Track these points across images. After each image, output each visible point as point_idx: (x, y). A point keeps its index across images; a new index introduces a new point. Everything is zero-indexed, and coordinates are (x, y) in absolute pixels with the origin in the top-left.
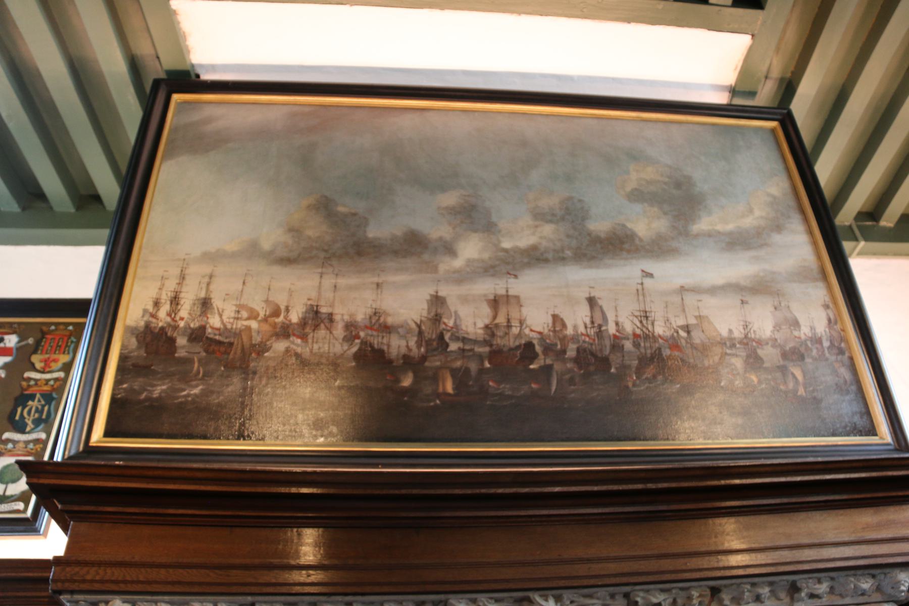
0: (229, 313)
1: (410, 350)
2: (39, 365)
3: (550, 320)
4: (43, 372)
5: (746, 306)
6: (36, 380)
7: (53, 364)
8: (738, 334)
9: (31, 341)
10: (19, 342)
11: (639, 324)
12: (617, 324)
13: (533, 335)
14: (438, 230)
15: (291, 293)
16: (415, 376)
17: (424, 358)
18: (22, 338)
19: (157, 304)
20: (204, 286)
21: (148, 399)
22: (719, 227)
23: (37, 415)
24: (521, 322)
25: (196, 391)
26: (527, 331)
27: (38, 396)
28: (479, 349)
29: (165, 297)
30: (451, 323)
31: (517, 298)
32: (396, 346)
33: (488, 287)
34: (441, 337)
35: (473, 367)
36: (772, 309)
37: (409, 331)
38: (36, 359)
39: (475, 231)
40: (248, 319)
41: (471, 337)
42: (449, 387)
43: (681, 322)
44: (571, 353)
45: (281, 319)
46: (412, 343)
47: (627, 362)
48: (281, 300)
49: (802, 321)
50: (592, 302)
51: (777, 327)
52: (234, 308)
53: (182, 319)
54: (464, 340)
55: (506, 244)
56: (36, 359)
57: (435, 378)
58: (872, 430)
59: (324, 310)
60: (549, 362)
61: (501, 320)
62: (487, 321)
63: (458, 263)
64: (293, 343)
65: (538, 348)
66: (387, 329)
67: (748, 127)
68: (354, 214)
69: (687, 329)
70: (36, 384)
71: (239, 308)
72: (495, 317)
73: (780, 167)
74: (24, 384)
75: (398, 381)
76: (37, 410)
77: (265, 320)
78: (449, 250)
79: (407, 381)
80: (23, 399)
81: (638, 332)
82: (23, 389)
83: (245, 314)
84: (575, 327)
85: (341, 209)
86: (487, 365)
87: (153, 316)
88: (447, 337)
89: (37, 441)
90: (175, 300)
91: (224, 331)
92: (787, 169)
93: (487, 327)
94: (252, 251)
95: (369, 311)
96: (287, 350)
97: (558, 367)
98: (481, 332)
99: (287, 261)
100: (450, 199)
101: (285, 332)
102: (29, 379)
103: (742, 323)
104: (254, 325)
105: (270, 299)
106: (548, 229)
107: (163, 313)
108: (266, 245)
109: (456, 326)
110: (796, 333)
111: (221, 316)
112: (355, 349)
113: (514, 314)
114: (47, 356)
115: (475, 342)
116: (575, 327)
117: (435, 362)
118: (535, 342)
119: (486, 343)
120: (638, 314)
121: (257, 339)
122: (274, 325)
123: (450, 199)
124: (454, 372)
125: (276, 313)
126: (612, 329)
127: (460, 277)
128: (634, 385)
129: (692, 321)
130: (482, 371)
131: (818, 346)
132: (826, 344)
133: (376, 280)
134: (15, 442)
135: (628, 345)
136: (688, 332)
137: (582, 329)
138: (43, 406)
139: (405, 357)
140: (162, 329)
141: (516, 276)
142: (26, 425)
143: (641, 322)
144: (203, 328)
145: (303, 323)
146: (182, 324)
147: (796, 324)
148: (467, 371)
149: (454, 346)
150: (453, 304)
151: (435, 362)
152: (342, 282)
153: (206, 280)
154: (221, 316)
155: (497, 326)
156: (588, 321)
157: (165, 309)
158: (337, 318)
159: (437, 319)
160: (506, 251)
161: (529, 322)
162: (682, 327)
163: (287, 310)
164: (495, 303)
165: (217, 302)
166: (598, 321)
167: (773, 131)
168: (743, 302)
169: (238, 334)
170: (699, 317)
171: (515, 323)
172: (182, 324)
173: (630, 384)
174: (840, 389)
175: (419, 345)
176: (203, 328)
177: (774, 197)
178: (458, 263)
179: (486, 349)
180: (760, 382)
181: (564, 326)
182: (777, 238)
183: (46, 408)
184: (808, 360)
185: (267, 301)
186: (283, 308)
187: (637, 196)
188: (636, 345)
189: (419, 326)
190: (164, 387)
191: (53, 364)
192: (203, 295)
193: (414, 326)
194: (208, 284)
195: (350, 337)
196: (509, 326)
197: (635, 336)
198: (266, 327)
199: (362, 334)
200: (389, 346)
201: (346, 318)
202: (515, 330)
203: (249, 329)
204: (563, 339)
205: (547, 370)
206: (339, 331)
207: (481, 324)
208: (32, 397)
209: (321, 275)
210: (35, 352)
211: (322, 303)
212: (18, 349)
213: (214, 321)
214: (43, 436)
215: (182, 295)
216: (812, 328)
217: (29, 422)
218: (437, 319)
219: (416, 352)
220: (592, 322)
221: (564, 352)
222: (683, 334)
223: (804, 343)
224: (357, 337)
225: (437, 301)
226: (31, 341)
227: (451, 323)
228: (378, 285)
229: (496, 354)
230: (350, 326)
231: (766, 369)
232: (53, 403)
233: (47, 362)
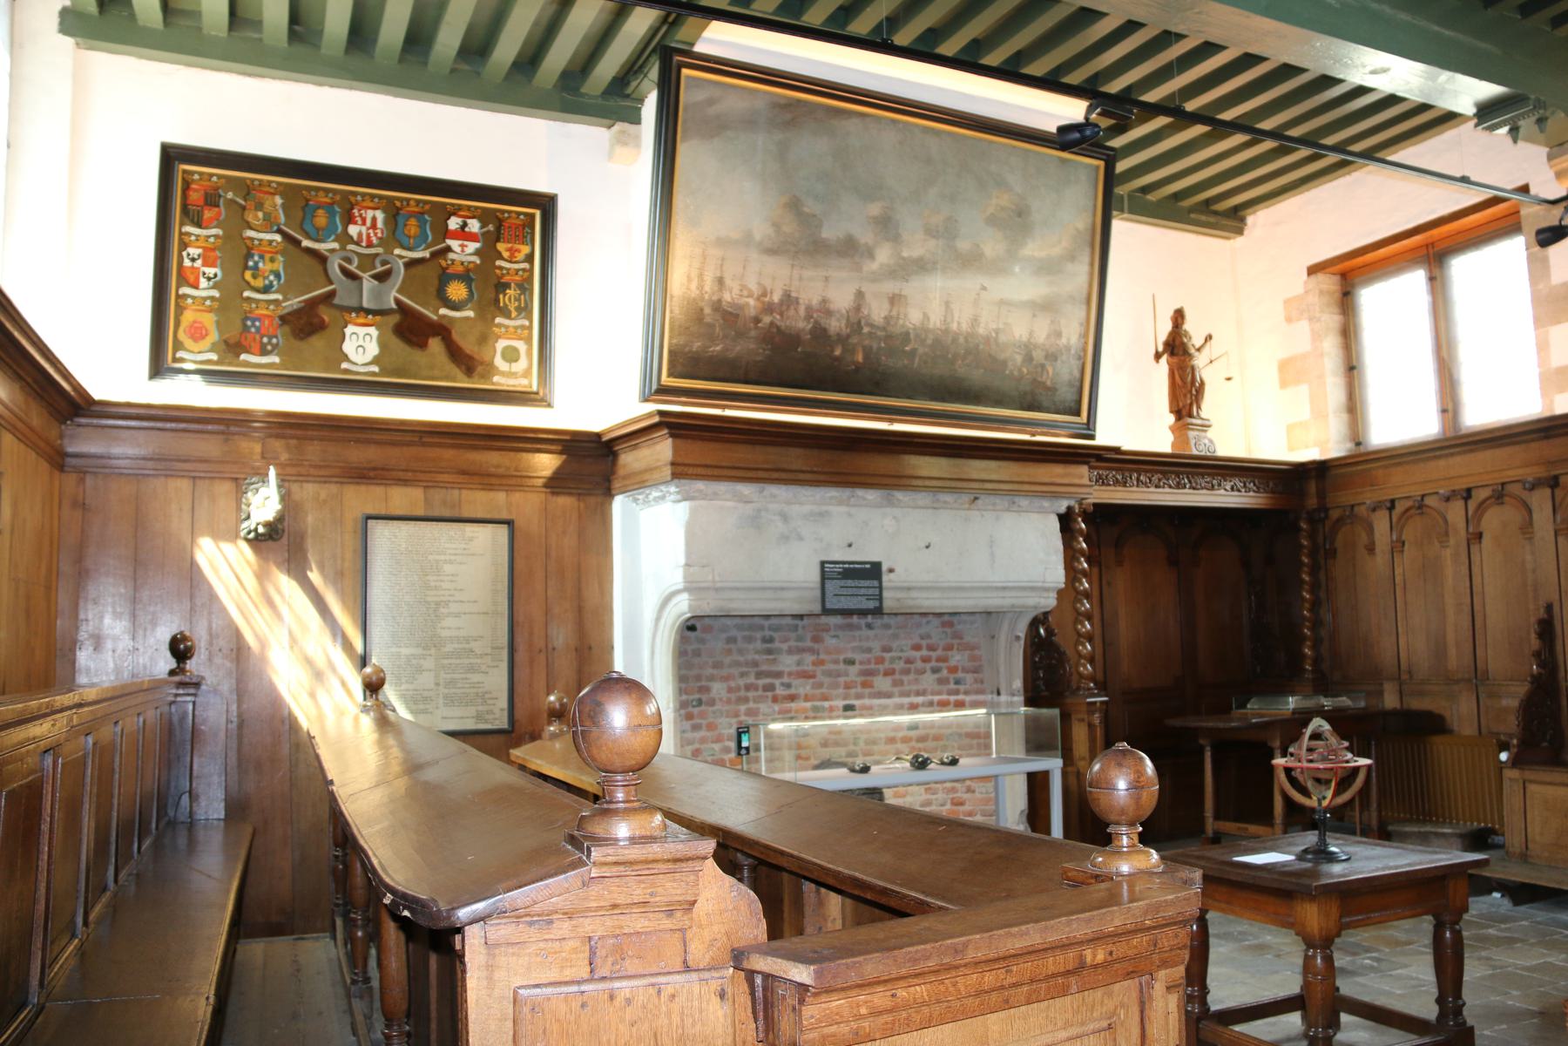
0: (736, 291)
1: (841, 330)
2: (506, 255)
3: (921, 316)
4: (511, 262)
6: (508, 269)
7: (516, 254)
8: (1024, 339)
9: (491, 227)
10: (482, 228)
13: (911, 326)
14: (865, 236)
15: (774, 278)
16: (843, 348)
17: (848, 336)
18: (484, 225)
21: (690, 352)
22: (1036, 254)
23: (517, 304)
24: (906, 315)
25: (718, 348)
27: (513, 285)
28: (880, 333)
30: (866, 313)
31: (905, 297)
32: (835, 325)
33: (890, 287)
34: (859, 322)
35: (875, 346)
36: (1049, 322)
37: (842, 315)
38: (501, 247)
39: (888, 240)
40: (747, 297)
41: (876, 323)
43: (994, 327)
44: (929, 342)
45: (767, 299)
46: (843, 325)
48: (768, 283)
49: (1064, 335)
51: (1048, 337)
52: (739, 287)
54: (872, 325)
55: (905, 254)
56: (501, 247)
57: (853, 352)
58: (1078, 413)
59: (793, 294)
61: (894, 313)
62: (886, 313)
63: (875, 266)
64: (774, 318)
65: (912, 336)
66: (829, 313)
67: (1081, 163)
68: (814, 216)
69: (997, 331)
70: (508, 273)
71: (743, 287)
72: (891, 311)
73: (1090, 204)
74: (497, 271)
75: (833, 351)
76: (516, 300)
77: (758, 299)
78: (870, 254)
79: (838, 352)
80: (502, 287)
82: (499, 278)
83: (745, 293)
84: (935, 323)
85: (806, 210)
86: (883, 345)
87: (688, 289)
88: (863, 323)
89: (523, 327)
91: (733, 304)
92: (1095, 206)
93: (886, 318)
94: (747, 240)
95: (820, 298)
96: (772, 323)
97: (921, 350)
98: (882, 320)
99: (772, 251)
100: (875, 209)
101: (769, 308)
102: (501, 268)
104: (752, 302)
105: (762, 282)
106: (932, 243)
107: (694, 285)
108: (758, 237)
109: (869, 315)
110: (1058, 342)
111: (731, 293)
112: (810, 326)
114: (510, 245)
115: (878, 328)
116: (935, 323)
117: (854, 340)
119: (884, 329)
121: (753, 313)
122: (763, 303)
123: (875, 209)
124: (864, 348)
125: (764, 294)
127: (875, 278)
129: (1001, 326)
130: (879, 348)
132: (1073, 352)
133: (825, 274)
134: (507, 327)
135: (961, 340)
136: (997, 333)
137: (938, 325)
138: (520, 295)
139: (838, 335)
141: (907, 281)
142: (510, 312)
144: (720, 301)
145: (781, 302)
146: (706, 297)
147: (1059, 334)
148: (871, 347)
149: (866, 330)
150: (868, 297)
151: (854, 340)
152: (808, 273)
153: (720, 262)
154: (731, 293)
155: (891, 317)
156: (943, 319)
158: (801, 301)
159: (858, 309)
160: (903, 258)
162: (994, 330)
163: (771, 293)
164: (894, 299)
165: (728, 282)
166: (949, 320)
167: (1097, 168)
168: (1034, 316)
169: (741, 307)
170: (1005, 324)
171: (902, 316)
172: (706, 297)
174: (1070, 384)
176: (720, 301)
177: (1077, 229)
178: (875, 266)
181: (928, 319)
182: (1070, 267)
183: (522, 297)
184: (1059, 362)
185: (759, 284)
186: (769, 290)
187: (992, 221)
188: (966, 341)
189: (847, 312)
190: (699, 344)
191: (516, 254)
193: (844, 311)
194: (722, 265)
195: (808, 317)
196: (898, 318)
197: (968, 333)
198: (759, 305)
199: (815, 315)
201: (807, 302)
202: (901, 322)
203: (748, 304)
204: (927, 331)
205: (914, 351)
207: (883, 316)
208: (507, 286)
209: (793, 266)
210: (498, 240)
211: (792, 289)
212: (483, 234)
213: (727, 297)
214: (527, 323)
216: (1069, 339)
217: (512, 309)
218: (858, 309)
219: (845, 331)
221: (925, 340)
222: (994, 335)
224: (812, 317)
225: (860, 295)
226: (491, 227)
227: (866, 313)
228: (827, 279)
229: (889, 337)
230: (809, 309)
232: (527, 293)
233: (512, 251)
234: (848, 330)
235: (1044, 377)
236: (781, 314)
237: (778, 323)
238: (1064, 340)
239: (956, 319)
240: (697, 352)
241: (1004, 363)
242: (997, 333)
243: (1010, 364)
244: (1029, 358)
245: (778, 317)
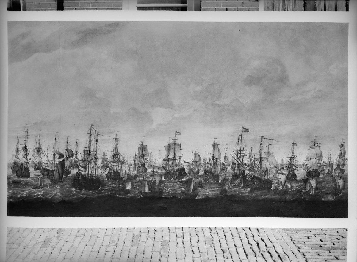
5: (295, 146)
11: (236, 158)
12: (225, 158)
17: (136, 176)
19: (17, 151)
20: (37, 141)
21: (22, 197)
26: (182, 162)
29: (21, 148)
42: (147, 190)
44: (201, 173)
47: (227, 178)
50: (215, 145)
51: (308, 159)
52: (53, 153)
53: (30, 159)
54: (154, 167)
60: (190, 177)
65: (187, 171)
75: (125, 187)
81: (235, 162)
90: (25, 149)
93: (164, 160)
103: (290, 156)
113: (177, 154)
118: (185, 167)
120: (236, 152)
126: (222, 160)
128: (229, 188)
131: (330, 168)
136: (260, 162)
137: (208, 161)
140: (22, 164)
143: (237, 157)
147: (320, 156)
148: (155, 182)
149: (149, 170)
155: (169, 159)
156: (211, 156)
157: (22, 153)
161: (184, 157)
163: (76, 154)
165: (44, 149)
171: (177, 158)
173: (227, 188)
175: (134, 170)
178: (154, 126)
179: (164, 171)
180: (292, 187)
181: (200, 159)
185: (67, 150)
186: (74, 152)
192: (38, 147)
199: (110, 165)
200: (121, 170)
202: (177, 162)
206: (100, 163)
207: (162, 159)
215: (28, 147)
216: (329, 159)
220: (213, 157)
221: (198, 172)
223: (321, 166)
224: (107, 166)
231: (297, 180)
234: (136, 172)
235: (308, 188)
236: (85, 167)
237: (83, 173)
238: (325, 160)
239: (223, 154)
240: (26, 197)
241: (270, 182)
242: (260, 162)
243: (274, 182)
244: (292, 177)
245: (83, 169)
